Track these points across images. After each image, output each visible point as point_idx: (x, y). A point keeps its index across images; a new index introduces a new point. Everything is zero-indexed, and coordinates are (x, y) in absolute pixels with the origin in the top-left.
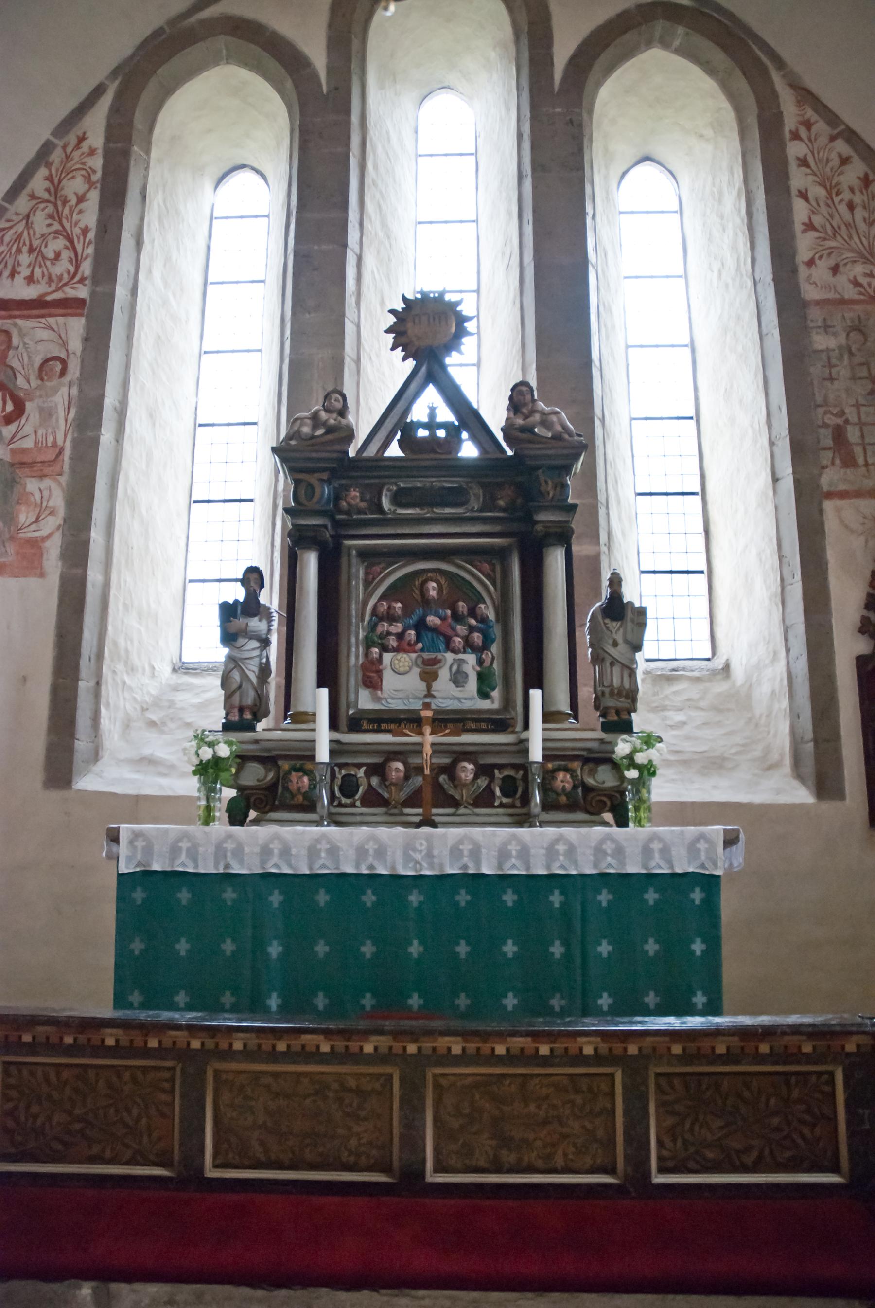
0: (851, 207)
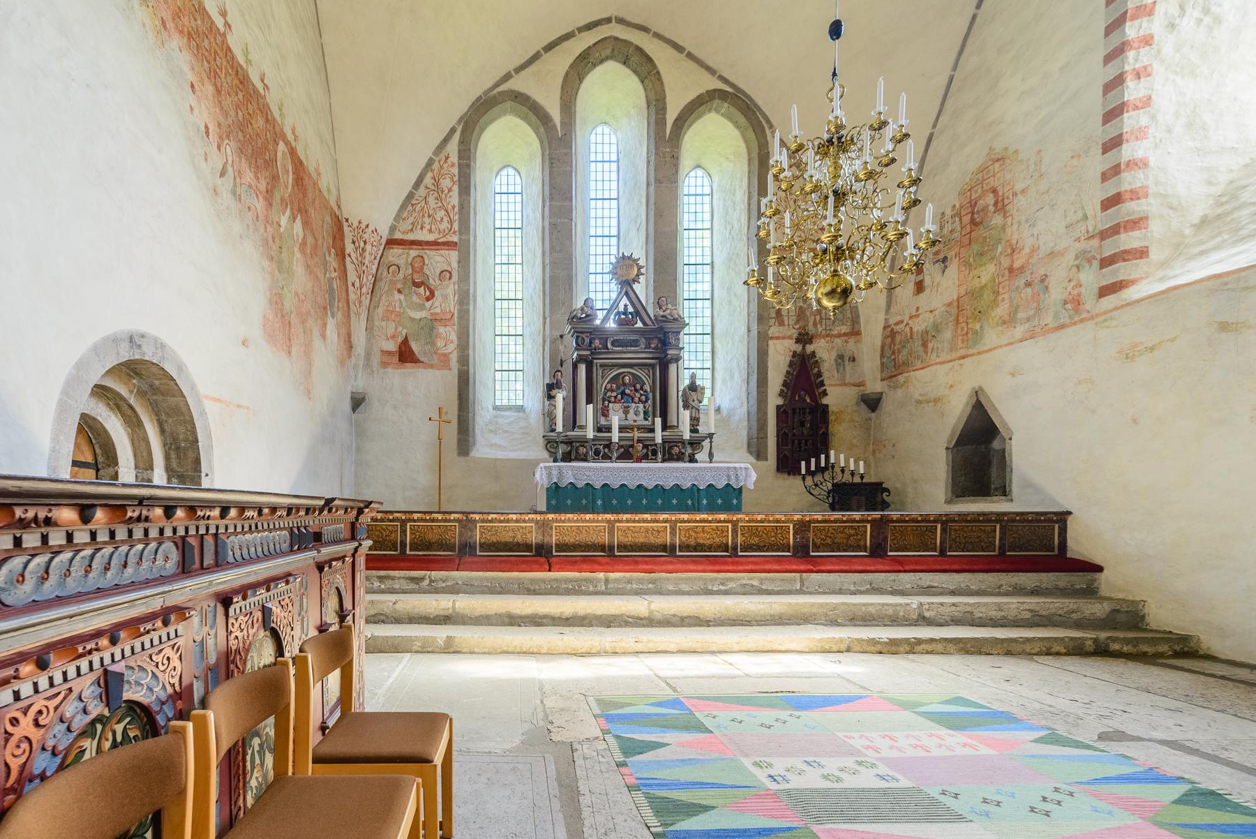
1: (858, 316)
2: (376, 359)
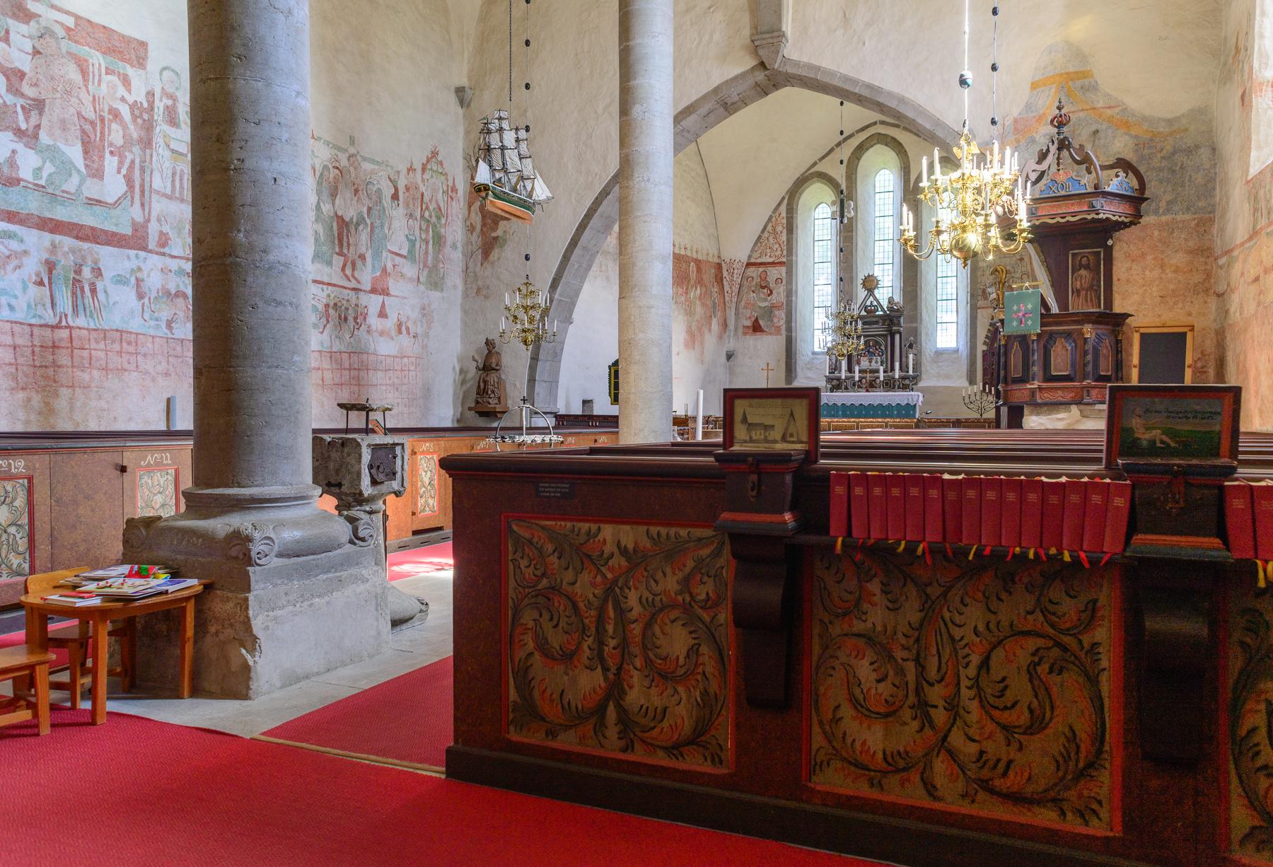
2: (740, 331)
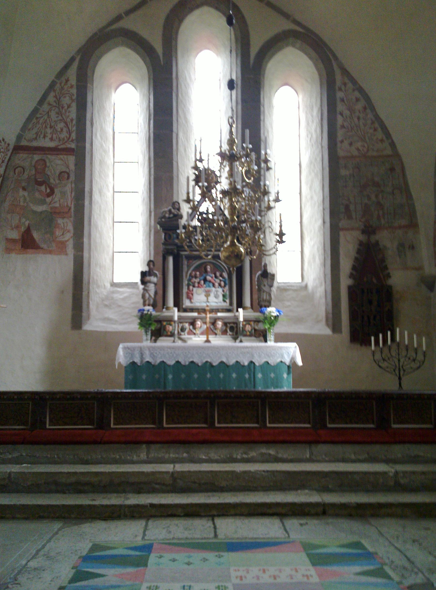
0: (359, 118)
1: (414, 212)
